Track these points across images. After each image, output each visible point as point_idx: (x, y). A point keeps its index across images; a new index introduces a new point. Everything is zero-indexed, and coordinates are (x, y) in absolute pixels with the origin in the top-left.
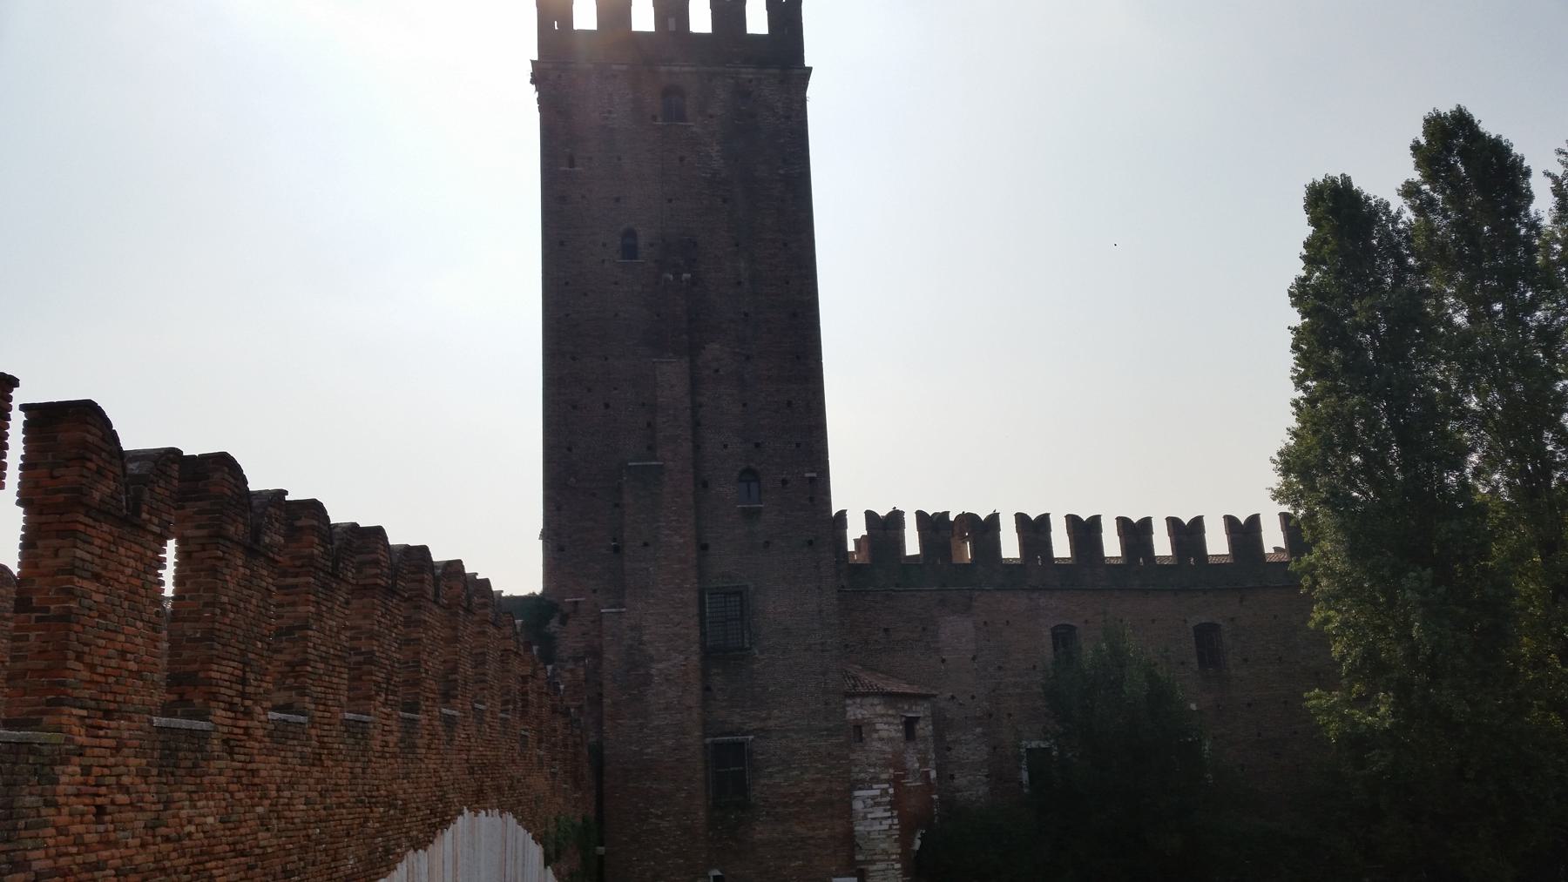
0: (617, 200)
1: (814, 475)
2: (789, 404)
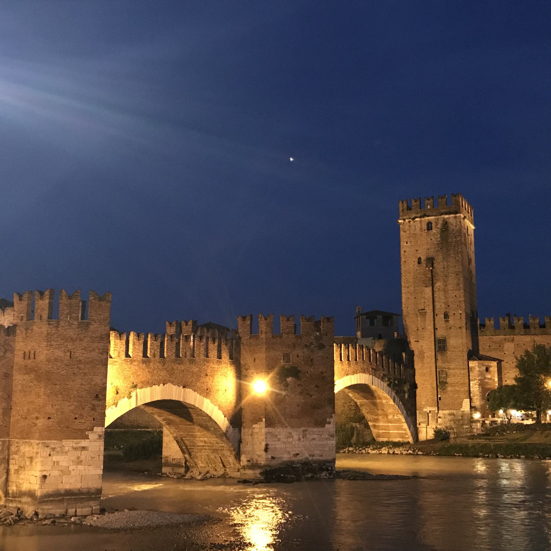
1: (461, 312)
2: (456, 296)
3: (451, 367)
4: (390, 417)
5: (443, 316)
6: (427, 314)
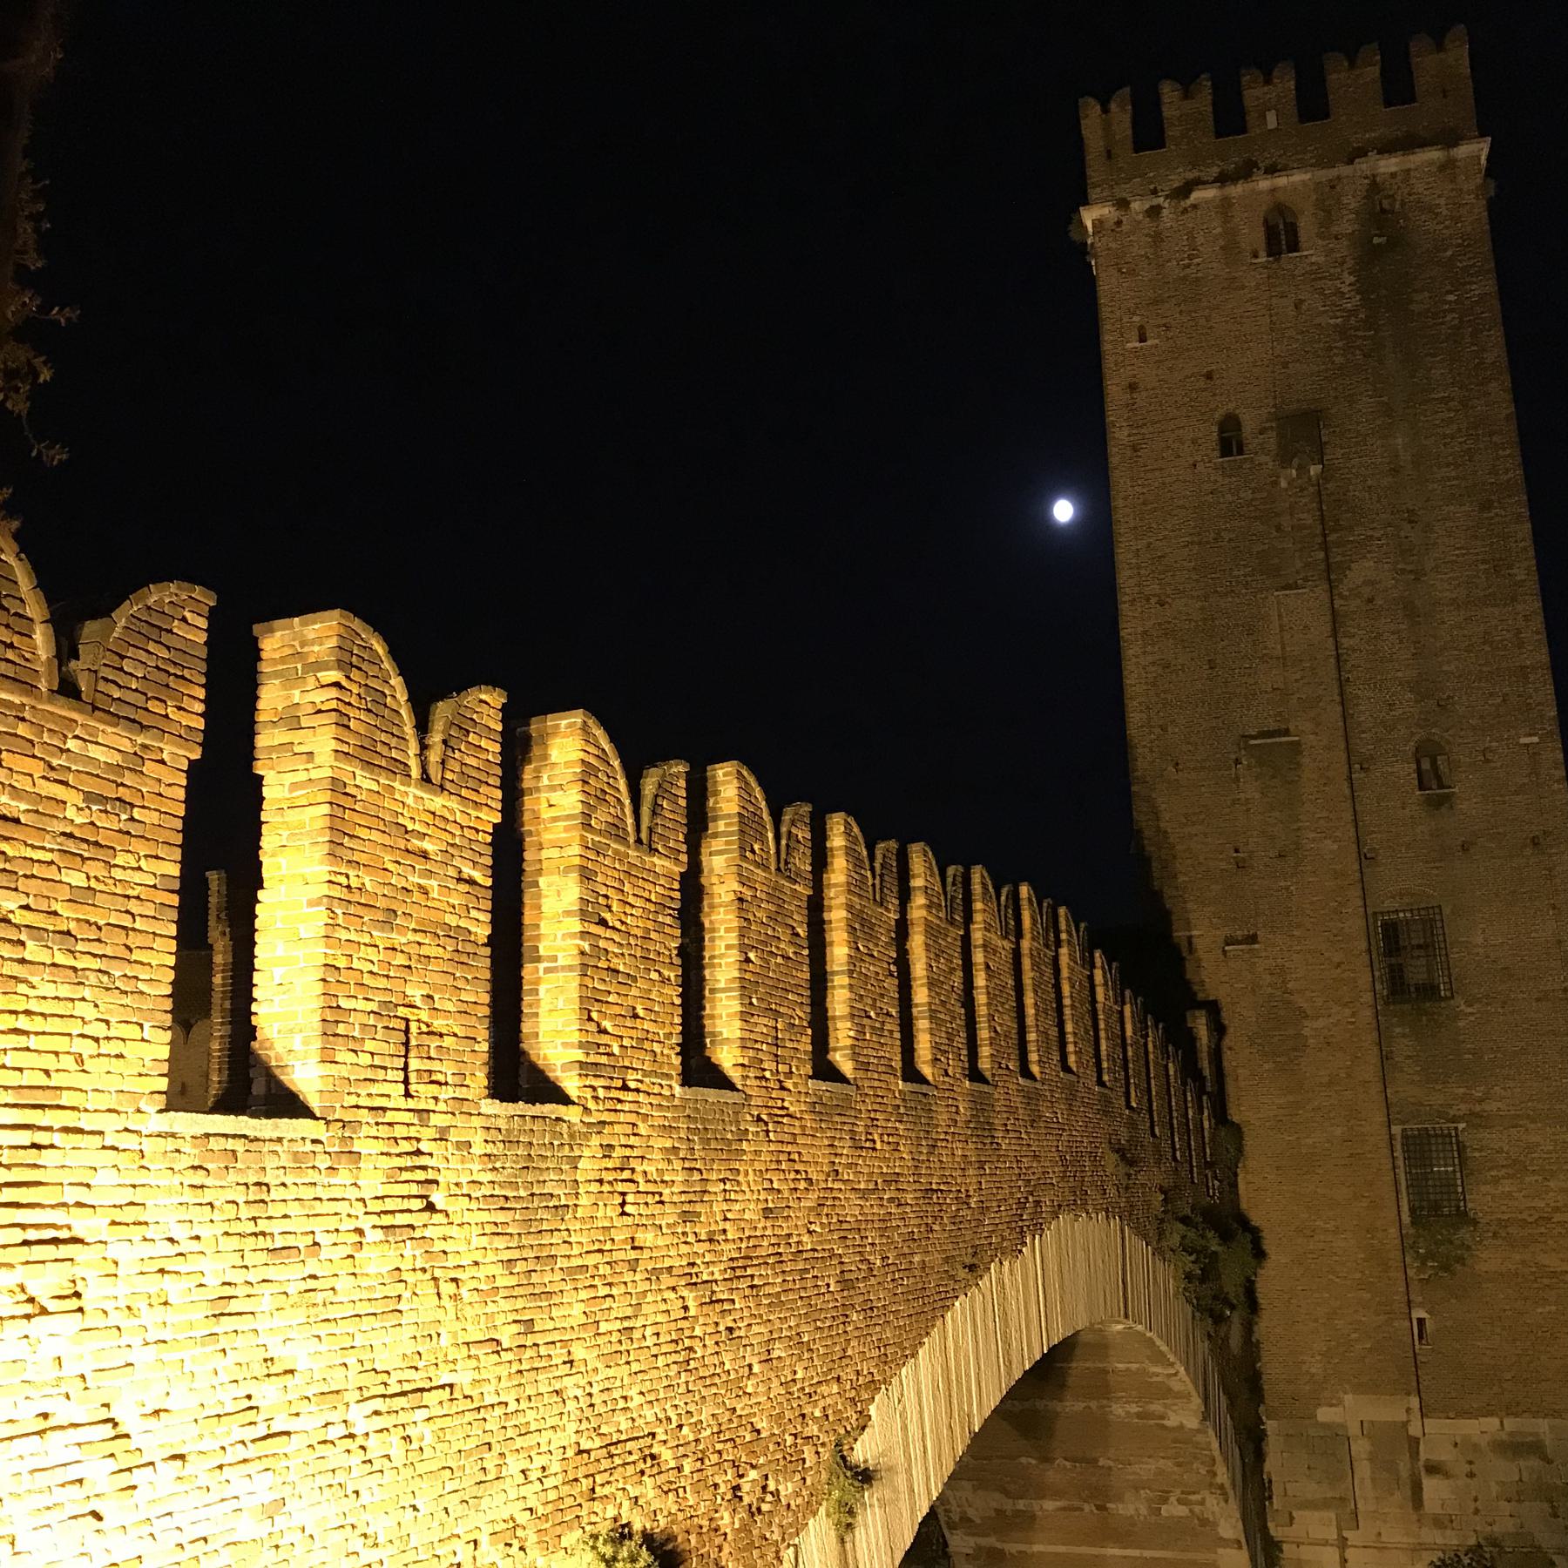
0: (1209, 376)
3: (1491, 1106)
4: (1129, 1508)
5: (1405, 771)
6: (1306, 760)
